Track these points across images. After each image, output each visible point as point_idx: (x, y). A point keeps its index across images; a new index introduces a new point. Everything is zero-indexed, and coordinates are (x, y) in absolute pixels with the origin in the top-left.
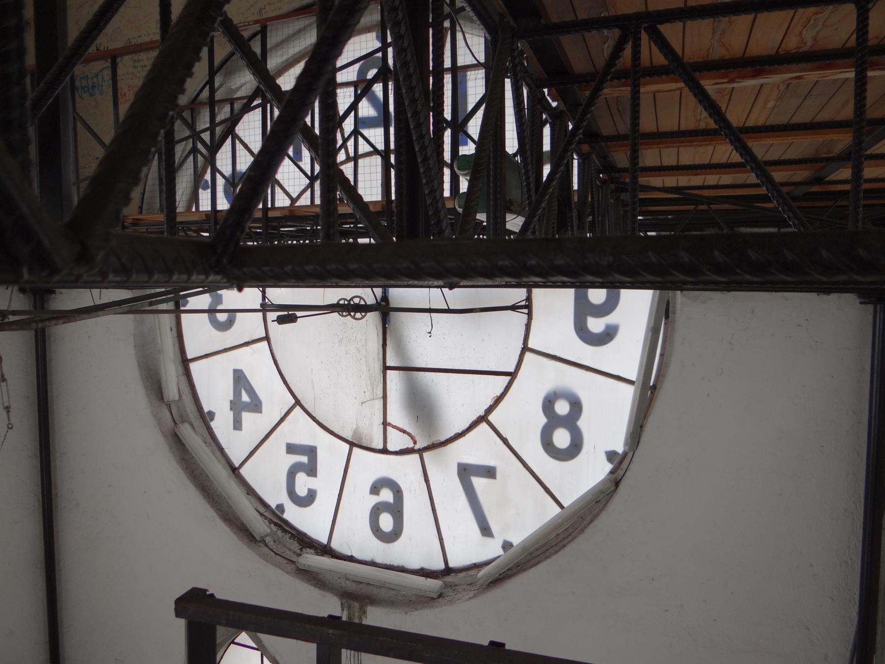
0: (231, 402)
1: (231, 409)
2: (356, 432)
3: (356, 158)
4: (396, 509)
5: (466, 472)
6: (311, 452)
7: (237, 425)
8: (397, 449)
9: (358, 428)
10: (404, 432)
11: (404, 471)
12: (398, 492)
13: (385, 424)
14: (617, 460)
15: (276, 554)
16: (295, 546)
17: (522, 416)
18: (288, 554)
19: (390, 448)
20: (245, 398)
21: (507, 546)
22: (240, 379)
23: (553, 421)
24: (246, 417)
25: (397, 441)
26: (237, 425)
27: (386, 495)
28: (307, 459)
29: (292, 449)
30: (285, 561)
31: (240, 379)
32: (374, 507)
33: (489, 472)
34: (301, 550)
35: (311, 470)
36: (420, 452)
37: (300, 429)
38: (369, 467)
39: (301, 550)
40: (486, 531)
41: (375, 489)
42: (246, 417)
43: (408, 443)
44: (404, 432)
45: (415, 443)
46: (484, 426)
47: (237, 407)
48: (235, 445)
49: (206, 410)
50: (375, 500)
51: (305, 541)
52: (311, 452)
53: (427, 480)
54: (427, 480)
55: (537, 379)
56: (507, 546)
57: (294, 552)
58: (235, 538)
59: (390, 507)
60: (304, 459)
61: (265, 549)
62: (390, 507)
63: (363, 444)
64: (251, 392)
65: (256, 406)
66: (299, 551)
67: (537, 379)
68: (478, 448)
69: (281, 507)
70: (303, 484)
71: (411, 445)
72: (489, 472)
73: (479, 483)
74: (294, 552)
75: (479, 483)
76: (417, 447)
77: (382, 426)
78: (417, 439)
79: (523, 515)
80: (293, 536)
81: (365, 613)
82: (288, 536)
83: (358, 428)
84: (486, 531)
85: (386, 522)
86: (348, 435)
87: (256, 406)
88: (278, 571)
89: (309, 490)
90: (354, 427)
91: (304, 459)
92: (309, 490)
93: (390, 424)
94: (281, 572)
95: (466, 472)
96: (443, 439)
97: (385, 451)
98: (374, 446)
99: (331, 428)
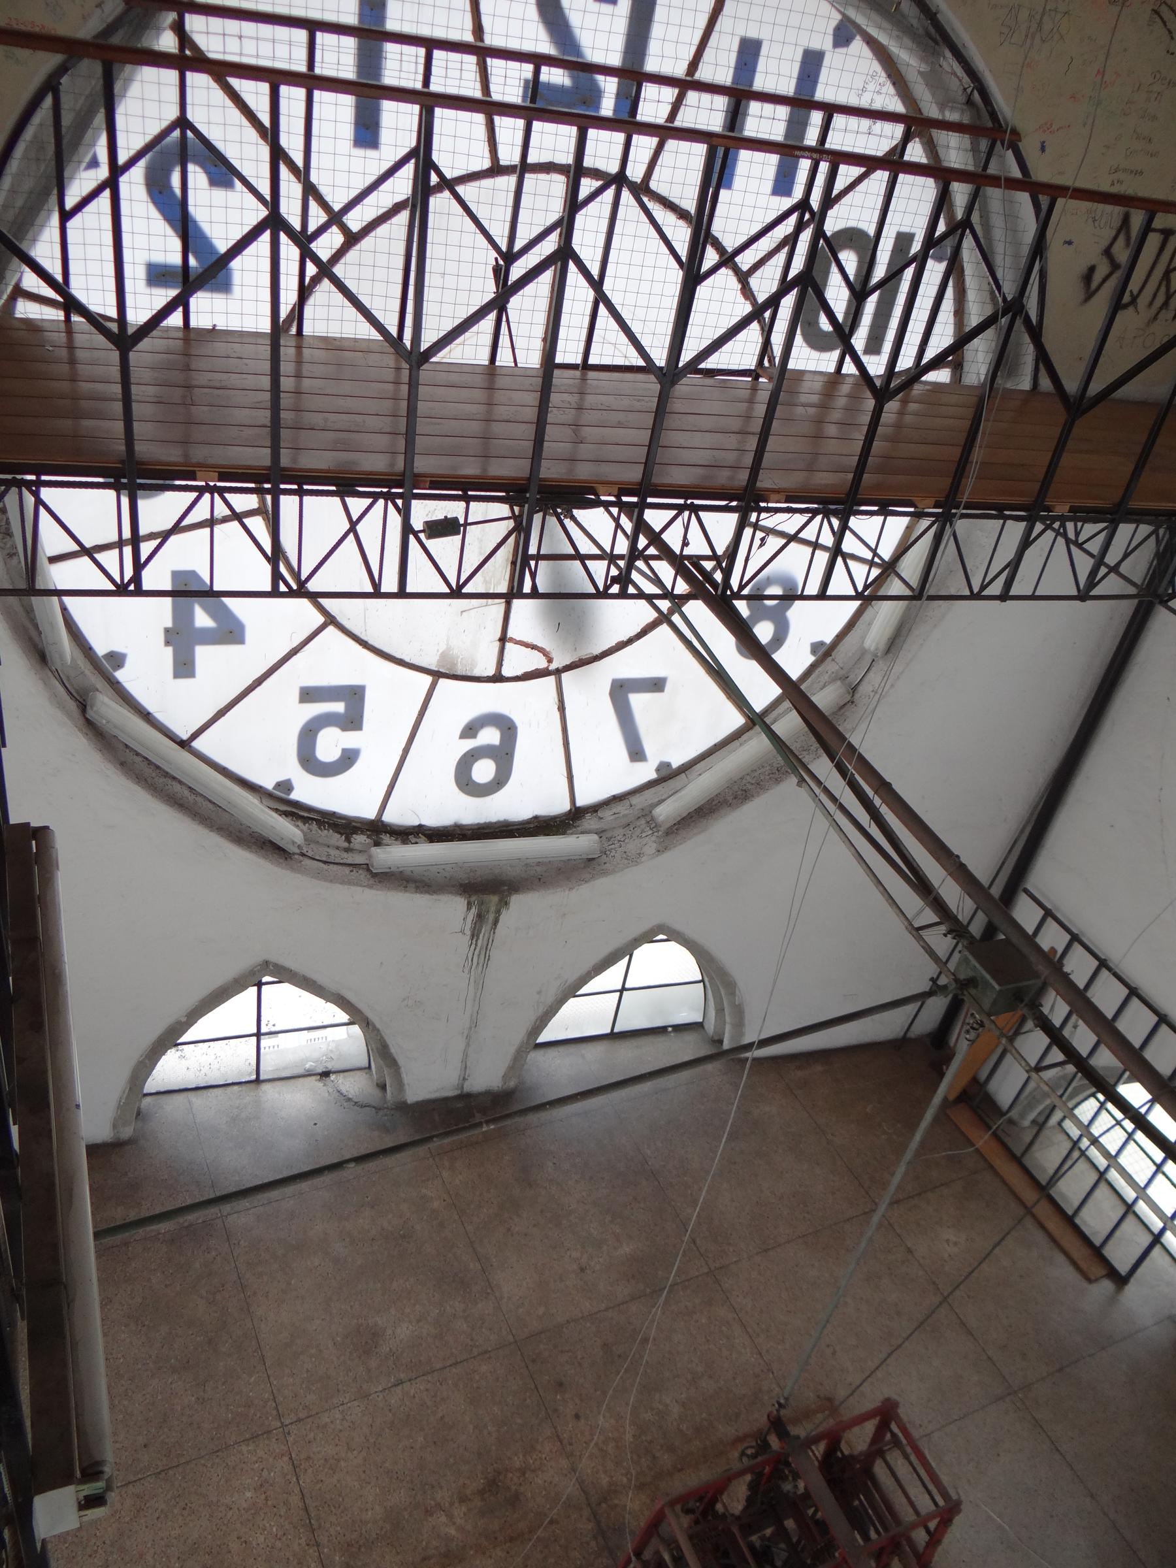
0: (167, 630)
2: (444, 656)
4: (504, 755)
5: (621, 691)
6: (354, 696)
7: (184, 667)
8: (519, 672)
9: (449, 649)
10: (534, 647)
11: (529, 705)
12: (508, 728)
13: (503, 639)
14: (820, 653)
15: (325, 862)
16: (338, 839)
18: (335, 855)
19: (506, 672)
24: (204, 654)
25: (518, 661)
26: (184, 667)
27: (490, 736)
28: (351, 705)
29: (308, 695)
30: (347, 870)
32: (465, 755)
33: (656, 685)
34: (348, 840)
35: (352, 721)
36: (558, 672)
37: (334, 663)
38: (460, 702)
39: (348, 840)
40: (636, 753)
42: (204, 654)
43: (537, 661)
44: (534, 647)
45: (550, 661)
48: (176, 703)
49: (101, 649)
51: (345, 826)
52: (354, 696)
53: (562, 708)
54: (562, 708)
57: (338, 848)
58: (261, 861)
60: (339, 707)
61: (307, 862)
63: (459, 673)
66: (346, 845)
69: (286, 786)
70: (330, 744)
71: (542, 663)
72: (656, 685)
73: (638, 701)
74: (338, 848)
75: (638, 701)
76: (553, 667)
77: (498, 644)
78: (553, 655)
80: (320, 823)
81: (506, 904)
82: (314, 826)
83: (449, 649)
84: (636, 753)
86: (431, 662)
87: (230, 632)
88: (353, 888)
89: (344, 750)
90: (443, 648)
91: (339, 707)
92: (344, 750)
93: (512, 640)
94: (360, 889)
95: (621, 691)
97: (498, 678)
98: (477, 672)
99: (398, 656)
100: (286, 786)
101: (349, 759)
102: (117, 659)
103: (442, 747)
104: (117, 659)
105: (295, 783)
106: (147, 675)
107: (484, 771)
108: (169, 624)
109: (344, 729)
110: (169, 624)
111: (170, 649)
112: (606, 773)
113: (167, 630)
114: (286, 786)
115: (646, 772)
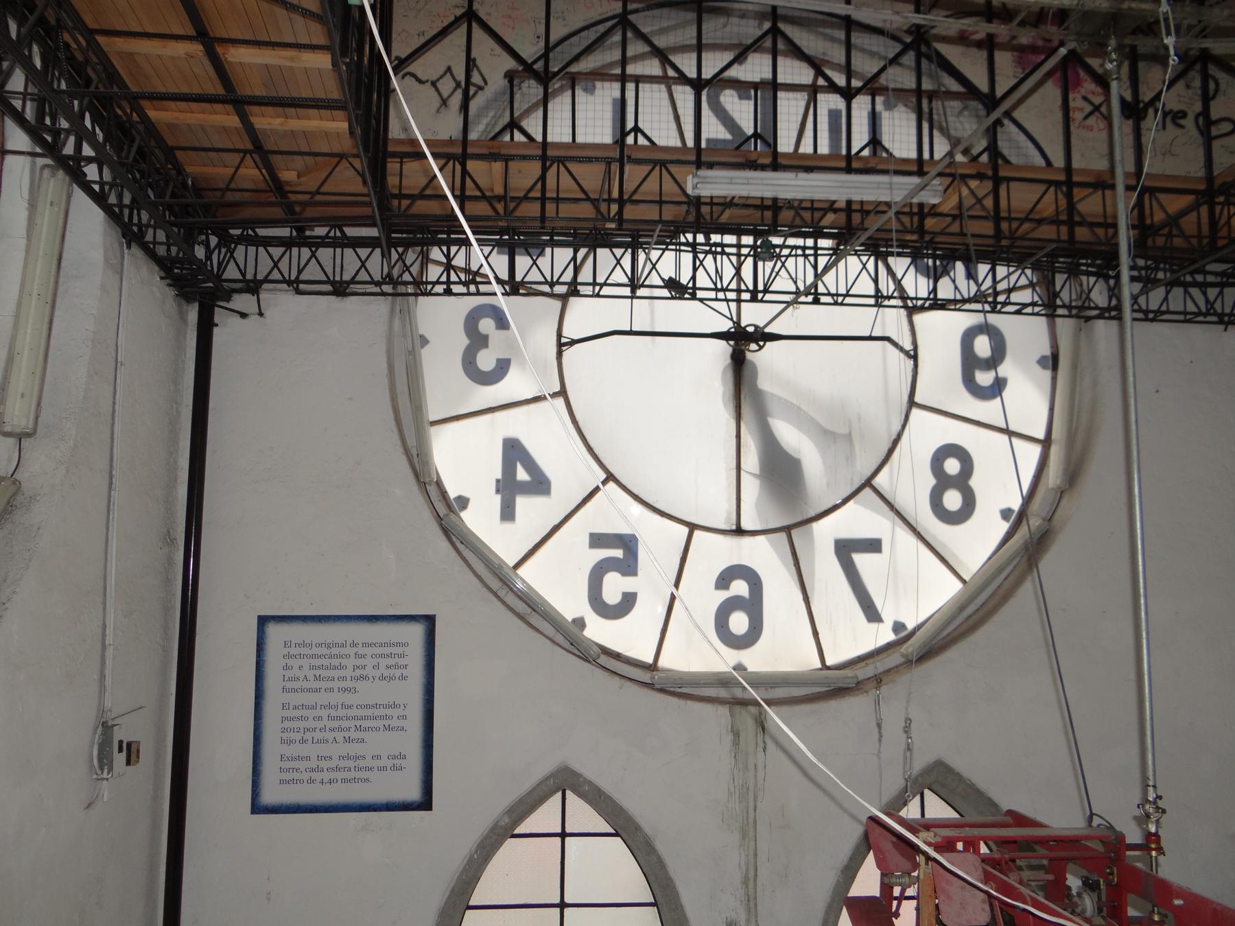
0: (498, 481)
1: (498, 491)
3: (276, 265)
4: (753, 605)
5: (846, 549)
6: (628, 543)
7: (508, 513)
17: (910, 479)
20: (522, 475)
21: (898, 627)
22: (514, 451)
23: (943, 482)
26: (508, 513)
27: (740, 588)
29: (597, 540)
31: (514, 451)
33: (873, 546)
35: (628, 566)
37: (614, 514)
40: (872, 614)
41: (723, 581)
46: (867, 490)
47: (508, 489)
50: (723, 595)
52: (628, 543)
55: (927, 434)
56: (898, 627)
59: (743, 601)
60: (618, 553)
62: (743, 601)
64: (531, 466)
65: (540, 485)
67: (927, 434)
68: (858, 519)
72: (873, 546)
73: (862, 560)
75: (860, 559)
79: (919, 590)
84: (872, 614)
85: (739, 622)
87: (540, 485)
91: (618, 553)
95: (846, 549)
96: (812, 513)
100: (580, 623)
101: (629, 601)
102: (463, 502)
103: (701, 597)
104: (463, 502)
105: (587, 621)
106: (481, 520)
107: (739, 622)
108: (500, 477)
109: (624, 574)
110: (500, 477)
111: (499, 497)
112: (852, 638)
113: (498, 481)
114: (580, 623)
115: (884, 635)
